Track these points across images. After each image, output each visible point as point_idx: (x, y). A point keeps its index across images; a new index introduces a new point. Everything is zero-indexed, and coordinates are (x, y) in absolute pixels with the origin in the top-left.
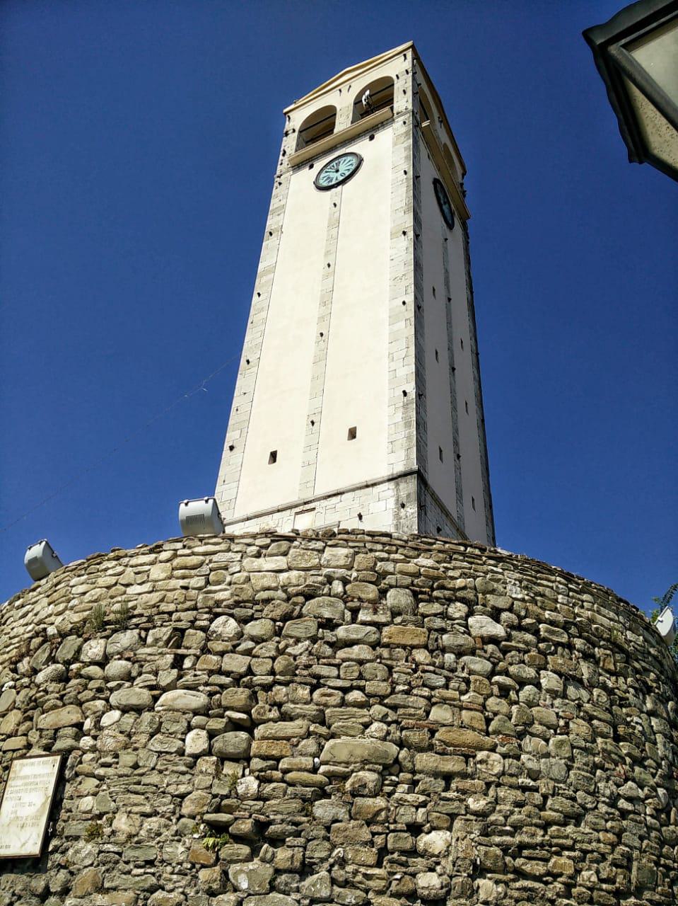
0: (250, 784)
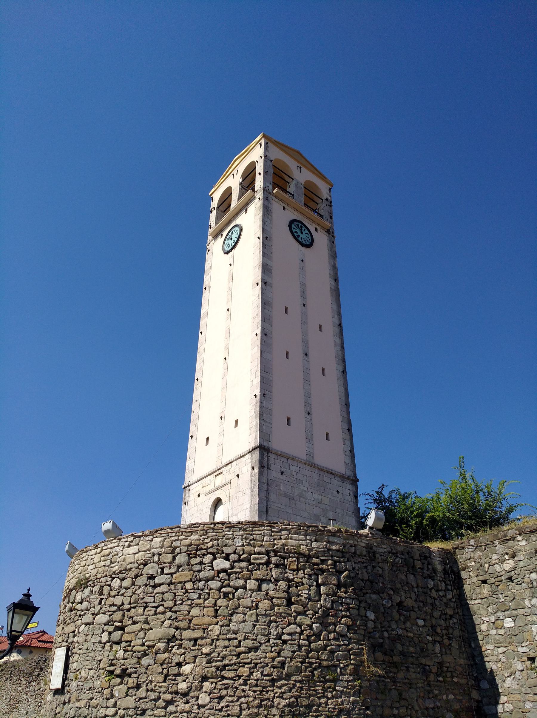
0: (121, 653)
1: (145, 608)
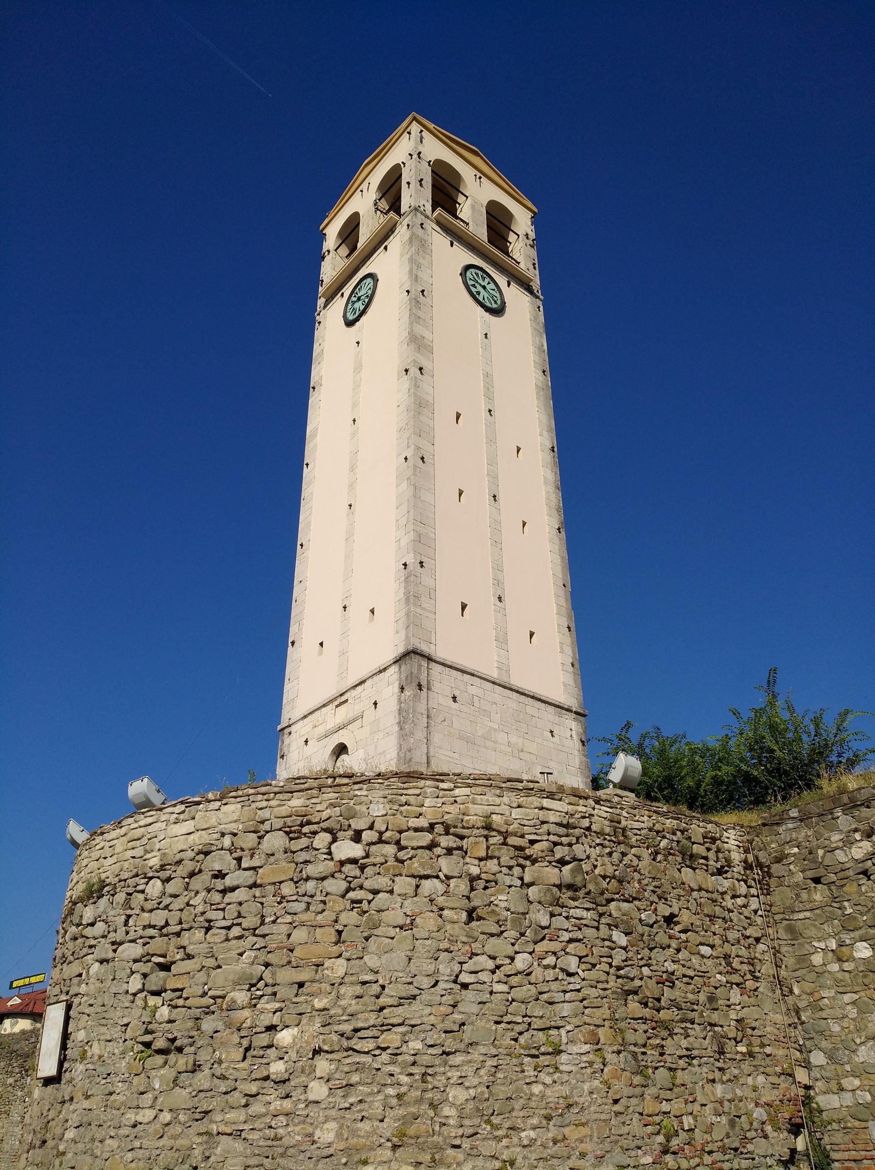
0: (164, 1012)
1: (208, 929)
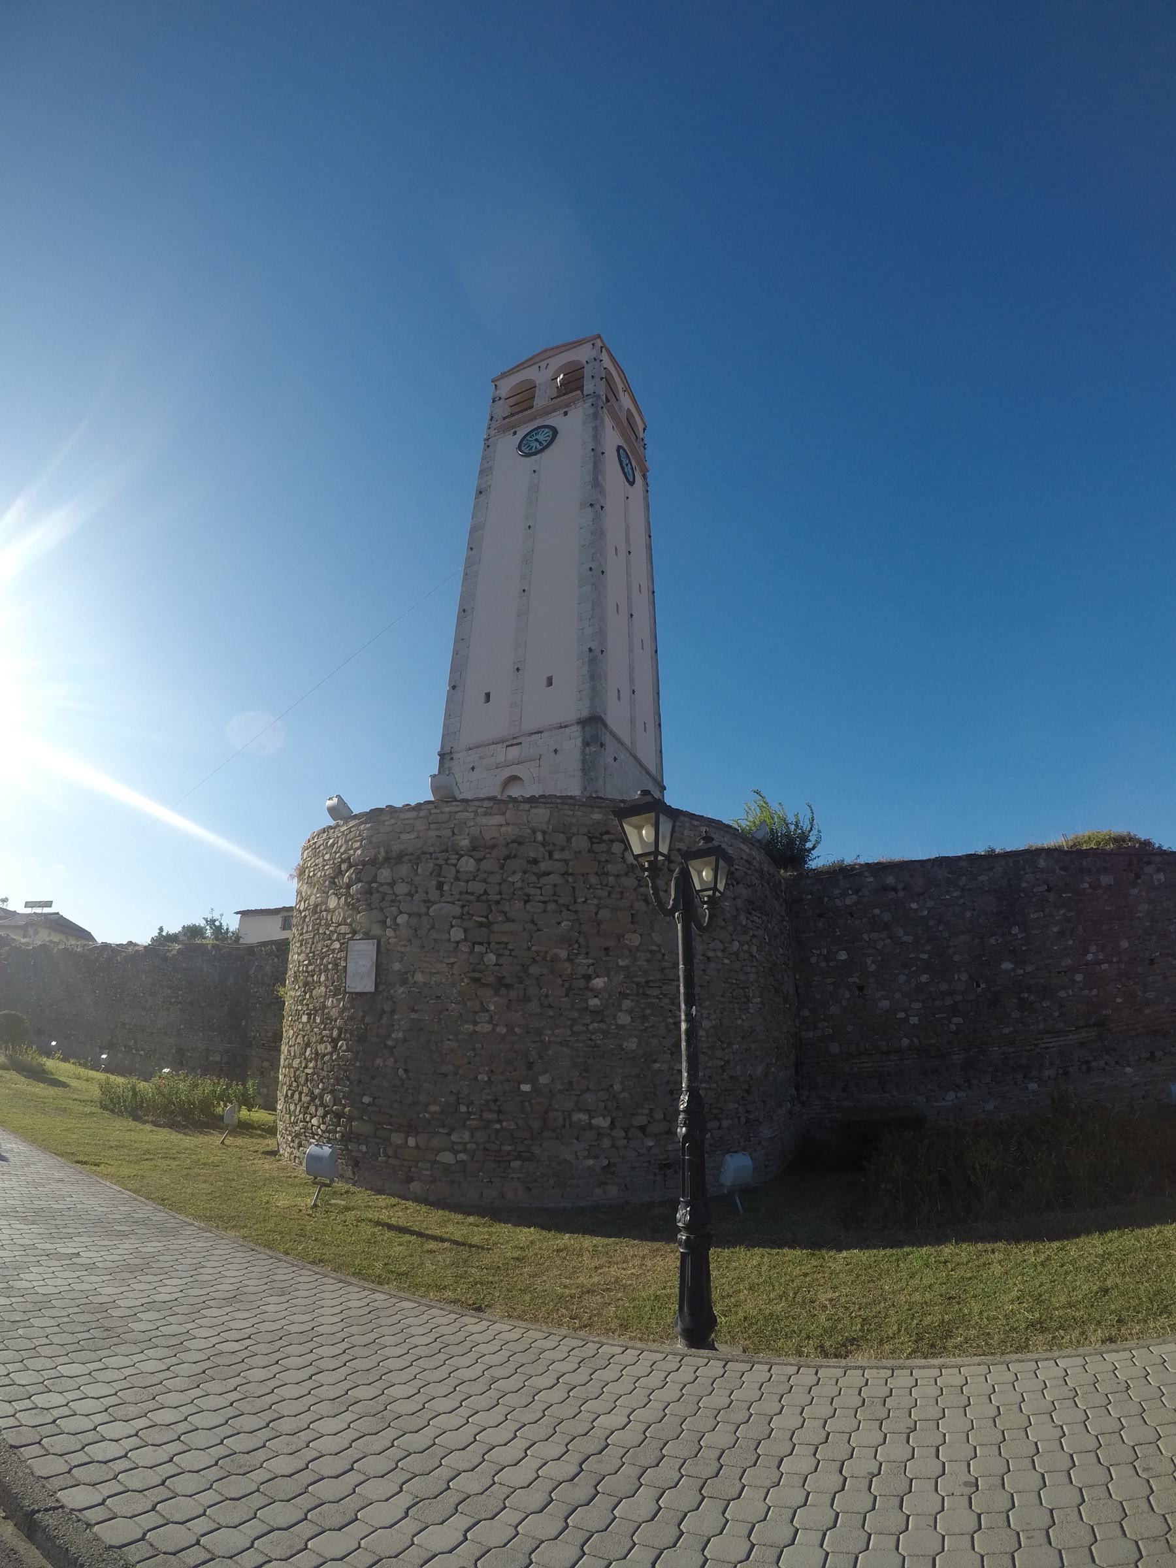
0: (491, 958)
1: (526, 902)
